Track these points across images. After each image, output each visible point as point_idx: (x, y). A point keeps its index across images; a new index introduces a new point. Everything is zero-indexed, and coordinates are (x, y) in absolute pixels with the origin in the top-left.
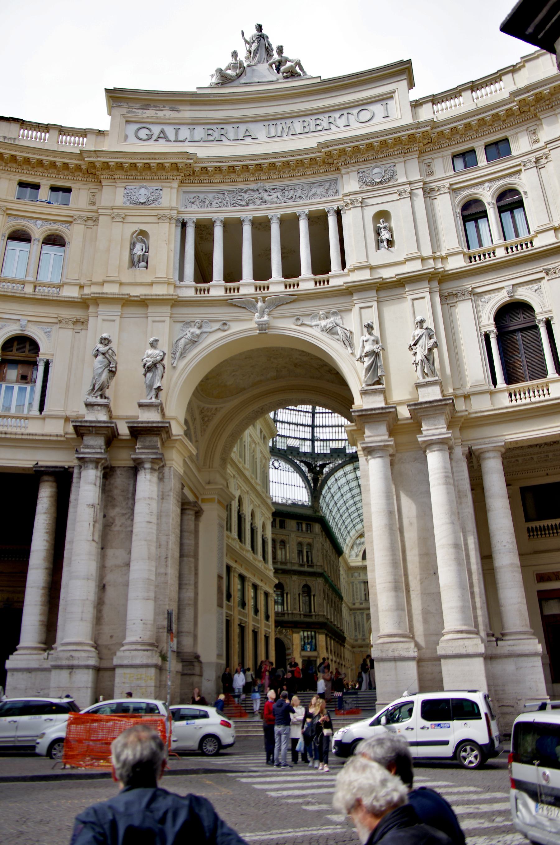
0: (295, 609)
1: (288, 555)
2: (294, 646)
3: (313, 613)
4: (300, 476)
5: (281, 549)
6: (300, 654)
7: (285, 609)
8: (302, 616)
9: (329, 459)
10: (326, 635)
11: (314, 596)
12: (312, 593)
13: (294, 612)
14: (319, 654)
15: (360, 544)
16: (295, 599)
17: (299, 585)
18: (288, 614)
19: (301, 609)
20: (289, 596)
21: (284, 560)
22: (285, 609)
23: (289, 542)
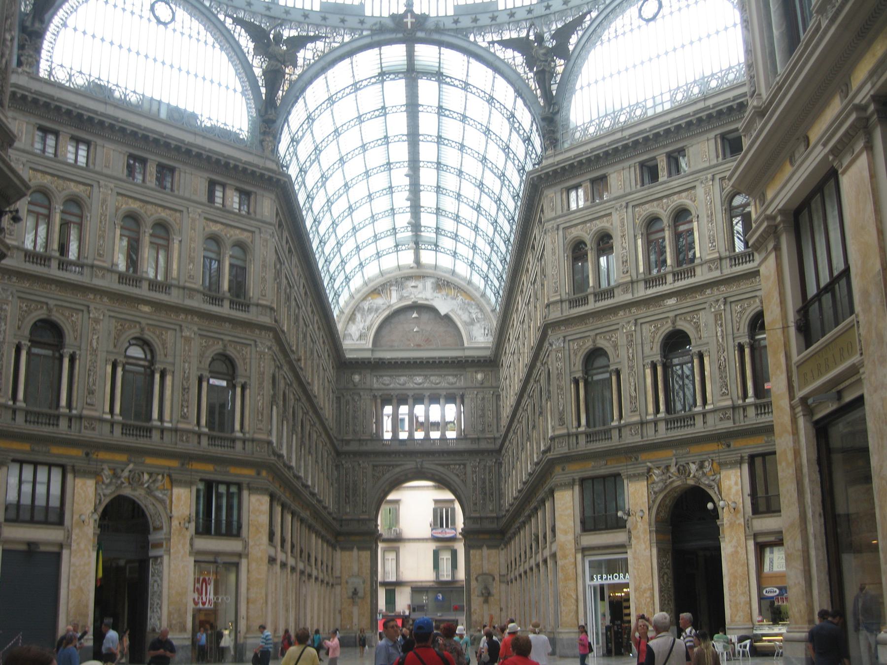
0: (184, 417)
1: (175, 266)
2: (175, 523)
3: (239, 435)
4: (230, 59)
5: (157, 247)
6: (191, 545)
7: (155, 415)
8: (204, 441)
9: (318, 26)
10: (272, 497)
11: (243, 388)
12: (240, 380)
13: (181, 426)
14: (246, 545)
15: (370, 310)
16: (185, 390)
17: (202, 355)
18: (162, 430)
19: (203, 421)
20: (168, 379)
21: (160, 278)
22: (155, 415)
23: (180, 231)
